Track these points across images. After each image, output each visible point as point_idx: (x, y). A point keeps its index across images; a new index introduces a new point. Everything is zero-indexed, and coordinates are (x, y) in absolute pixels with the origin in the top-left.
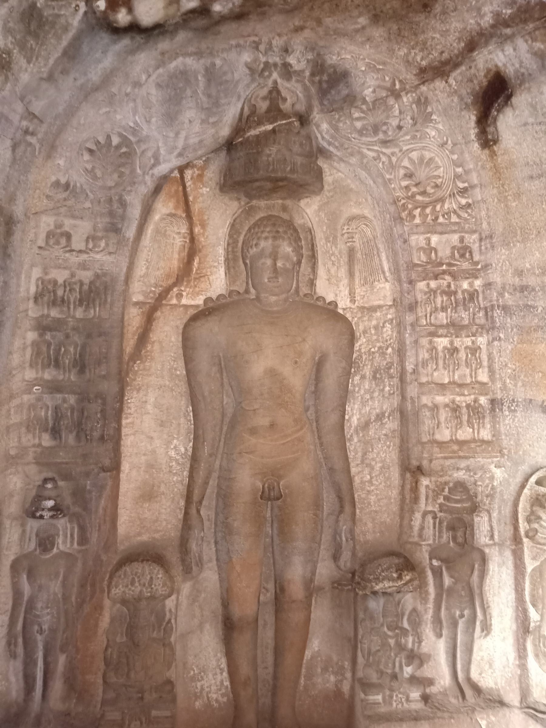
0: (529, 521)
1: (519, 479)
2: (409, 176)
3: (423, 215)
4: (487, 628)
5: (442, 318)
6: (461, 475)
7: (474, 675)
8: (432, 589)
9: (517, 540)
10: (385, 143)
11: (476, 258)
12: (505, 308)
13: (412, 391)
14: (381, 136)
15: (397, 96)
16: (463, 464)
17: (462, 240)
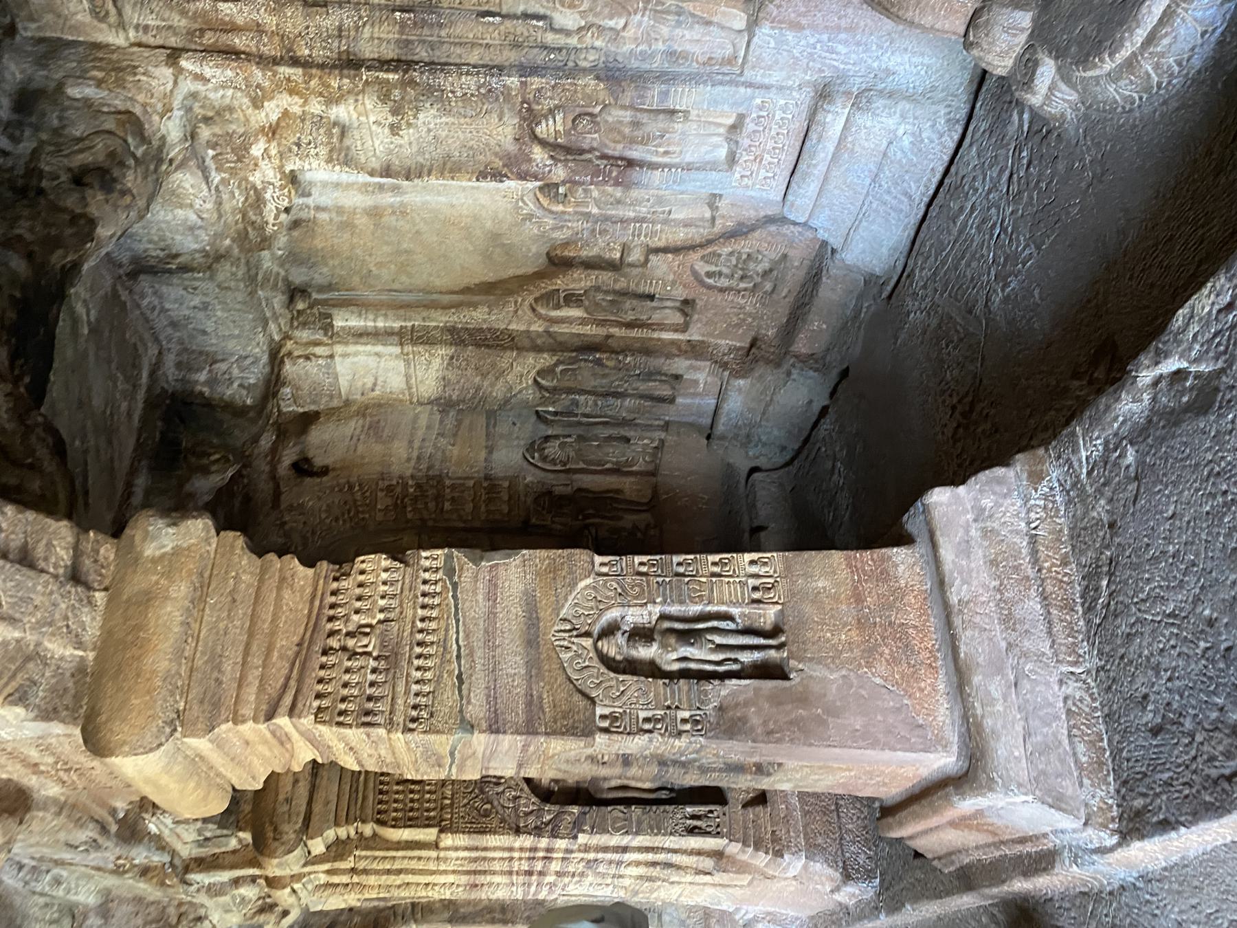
0: (555, 465)
1: (532, 468)
2: (337, 519)
3: (363, 512)
4: (618, 491)
5: (432, 505)
6: (529, 500)
7: (645, 500)
8: (597, 520)
9: (568, 471)
10: (313, 533)
11: (394, 482)
12: (429, 469)
13: (477, 524)
14: (309, 535)
15: (285, 523)
16: (522, 498)
17: (382, 490)
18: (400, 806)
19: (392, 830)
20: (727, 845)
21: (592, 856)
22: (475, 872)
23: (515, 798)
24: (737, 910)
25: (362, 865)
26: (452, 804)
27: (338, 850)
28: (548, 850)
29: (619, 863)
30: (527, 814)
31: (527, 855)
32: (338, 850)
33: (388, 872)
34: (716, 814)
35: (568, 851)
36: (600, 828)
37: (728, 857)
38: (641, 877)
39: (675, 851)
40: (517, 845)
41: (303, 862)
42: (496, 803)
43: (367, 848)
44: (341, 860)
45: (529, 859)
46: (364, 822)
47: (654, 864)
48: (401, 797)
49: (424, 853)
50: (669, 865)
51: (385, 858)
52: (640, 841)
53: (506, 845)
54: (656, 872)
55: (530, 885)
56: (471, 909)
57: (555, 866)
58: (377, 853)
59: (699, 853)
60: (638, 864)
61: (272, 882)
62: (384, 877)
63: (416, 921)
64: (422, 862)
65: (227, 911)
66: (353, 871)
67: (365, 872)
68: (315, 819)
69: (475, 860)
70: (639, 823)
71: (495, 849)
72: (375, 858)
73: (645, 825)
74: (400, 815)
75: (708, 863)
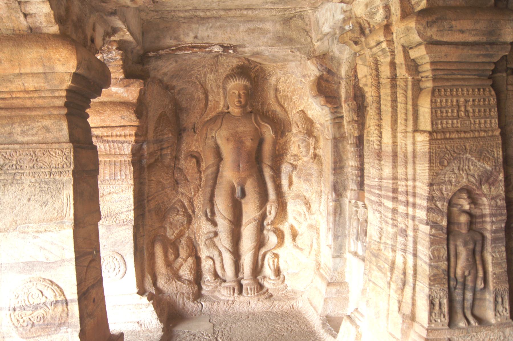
18: (444, 104)
19: (429, 100)
20: (423, 326)
21: (410, 233)
22: (395, 155)
23: (450, 182)
24: (362, 315)
25: (400, 83)
26: (446, 139)
27: (413, 66)
28: (414, 205)
29: (405, 251)
30: (441, 190)
31: (410, 190)
32: (413, 66)
33: (394, 100)
34: (443, 319)
35: (414, 218)
36: (433, 242)
37: (412, 325)
38: (393, 263)
39: (414, 288)
40: (418, 184)
41: (406, 45)
42: (447, 168)
43: (413, 85)
44: (406, 69)
45: (407, 192)
46: (434, 79)
47: (404, 273)
48: (449, 104)
49: (410, 123)
50: (404, 284)
51: (406, 97)
52: (424, 268)
53: (417, 177)
54: (398, 274)
55: (380, 189)
56: (341, 150)
57: (402, 209)
58: (410, 93)
59: (414, 305)
60: (405, 263)
61: (387, 28)
62: (389, 98)
63: (334, 119)
64: (403, 122)
65: (367, 5)
66: (394, 78)
67: (394, 86)
68: (438, 48)
69: (406, 156)
70: (437, 267)
71: (414, 169)
72: (406, 91)
73: (435, 271)
74: (438, 104)
75: (407, 309)
